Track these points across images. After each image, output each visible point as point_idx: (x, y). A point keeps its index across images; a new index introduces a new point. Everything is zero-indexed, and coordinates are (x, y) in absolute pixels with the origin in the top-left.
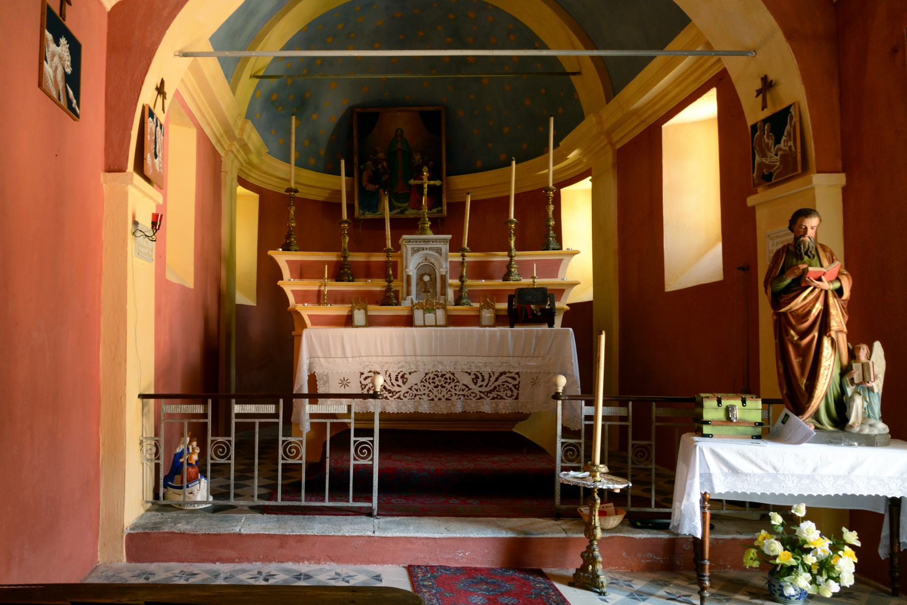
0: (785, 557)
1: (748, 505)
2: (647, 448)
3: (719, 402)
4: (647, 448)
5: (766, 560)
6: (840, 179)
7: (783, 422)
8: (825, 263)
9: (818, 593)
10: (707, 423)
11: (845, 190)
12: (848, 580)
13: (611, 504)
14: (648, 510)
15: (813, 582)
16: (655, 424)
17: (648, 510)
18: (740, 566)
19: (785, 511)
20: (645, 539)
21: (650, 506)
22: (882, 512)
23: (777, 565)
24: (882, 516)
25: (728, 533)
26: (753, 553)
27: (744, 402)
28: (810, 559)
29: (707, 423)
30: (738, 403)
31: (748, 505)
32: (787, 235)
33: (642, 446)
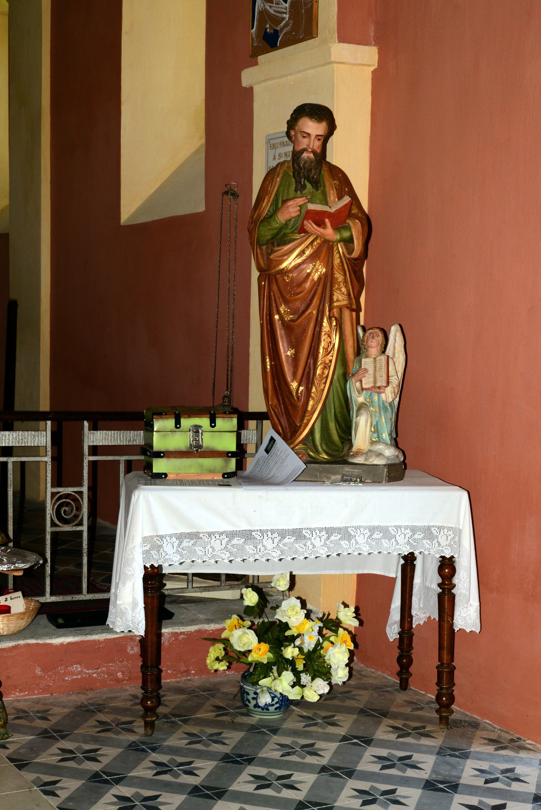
0: (261, 653)
1: (223, 578)
2: (76, 499)
3: (178, 423)
4: (76, 499)
5: (232, 656)
6: (368, 56)
7: (267, 451)
8: (332, 195)
9: (303, 697)
10: (159, 455)
11: (378, 78)
12: (340, 675)
13: (19, 594)
14: (77, 597)
15: (297, 683)
16: (88, 459)
17: (77, 597)
18: (203, 669)
19: (260, 587)
20: (69, 644)
21: (80, 592)
22: (393, 575)
23: (250, 664)
24: (394, 580)
25: (193, 622)
26: (216, 651)
27: (213, 423)
28: (290, 652)
29: (159, 455)
30: (204, 422)
31: (223, 578)
32: (283, 144)
33: (68, 496)
